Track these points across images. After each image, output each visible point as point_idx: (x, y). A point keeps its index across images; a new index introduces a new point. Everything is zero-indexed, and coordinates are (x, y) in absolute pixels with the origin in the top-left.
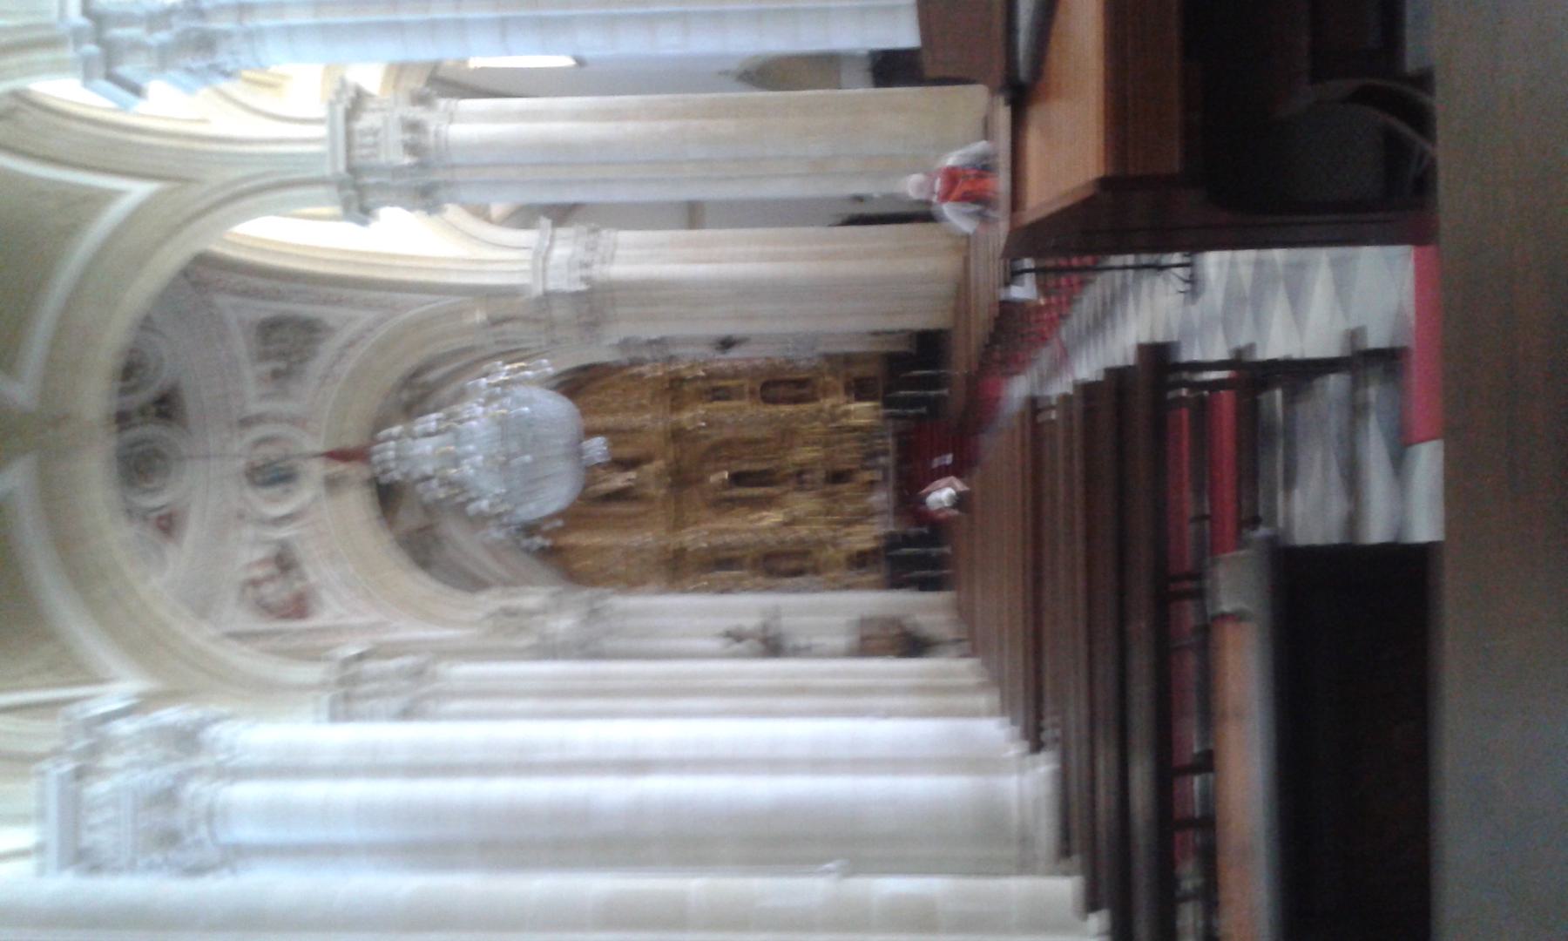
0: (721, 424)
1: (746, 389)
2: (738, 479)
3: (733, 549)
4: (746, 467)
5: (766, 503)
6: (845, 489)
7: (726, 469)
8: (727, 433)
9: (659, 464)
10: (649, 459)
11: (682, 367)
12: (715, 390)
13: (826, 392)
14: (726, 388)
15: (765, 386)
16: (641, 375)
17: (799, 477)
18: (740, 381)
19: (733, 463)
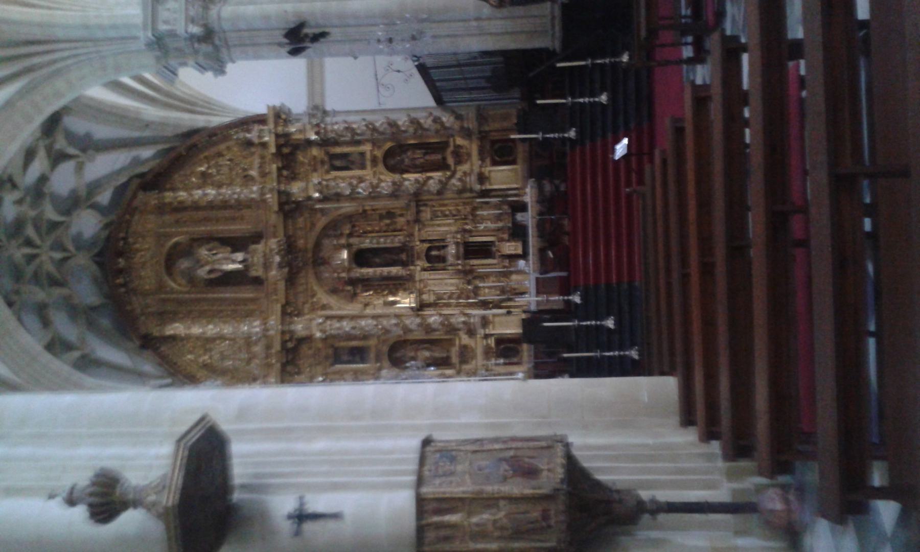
0: (338, 197)
1: (368, 156)
2: (361, 258)
3: (355, 338)
4: (367, 243)
5: (396, 285)
6: (479, 264)
7: (343, 247)
8: (347, 207)
9: (273, 243)
10: (257, 237)
11: (293, 129)
12: (333, 157)
13: (460, 156)
14: (344, 156)
15: (388, 155)
16: (249, 144)
17: (435, 260)
18: (362, 148)
19: (353, 240)
